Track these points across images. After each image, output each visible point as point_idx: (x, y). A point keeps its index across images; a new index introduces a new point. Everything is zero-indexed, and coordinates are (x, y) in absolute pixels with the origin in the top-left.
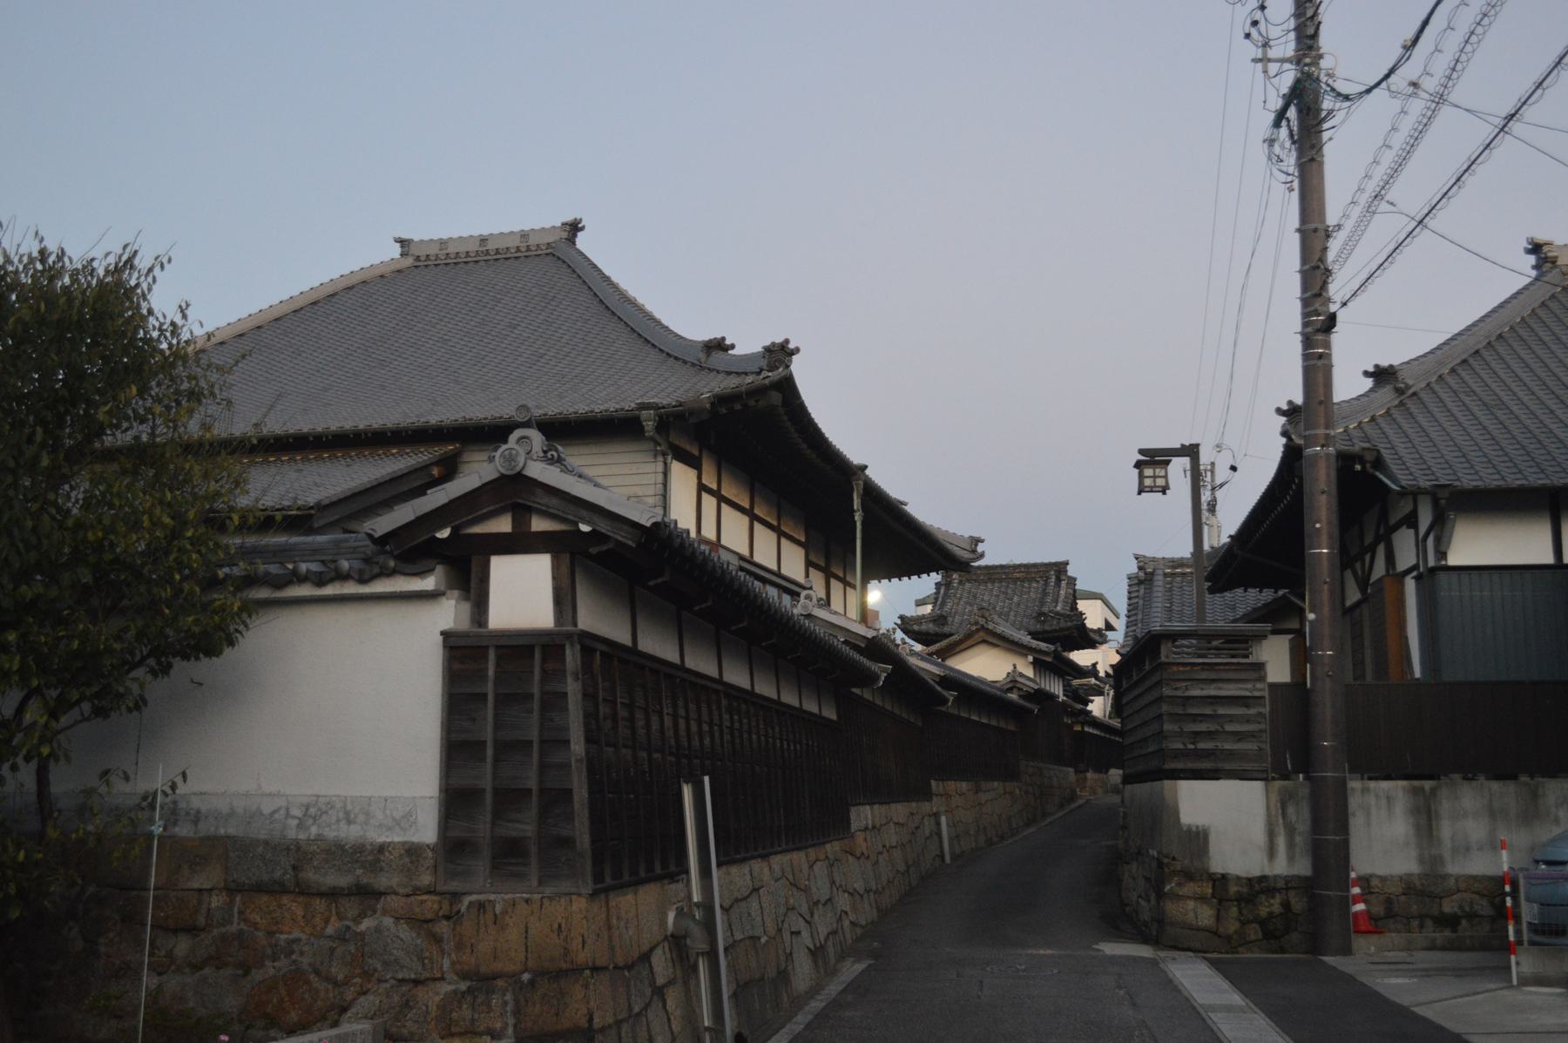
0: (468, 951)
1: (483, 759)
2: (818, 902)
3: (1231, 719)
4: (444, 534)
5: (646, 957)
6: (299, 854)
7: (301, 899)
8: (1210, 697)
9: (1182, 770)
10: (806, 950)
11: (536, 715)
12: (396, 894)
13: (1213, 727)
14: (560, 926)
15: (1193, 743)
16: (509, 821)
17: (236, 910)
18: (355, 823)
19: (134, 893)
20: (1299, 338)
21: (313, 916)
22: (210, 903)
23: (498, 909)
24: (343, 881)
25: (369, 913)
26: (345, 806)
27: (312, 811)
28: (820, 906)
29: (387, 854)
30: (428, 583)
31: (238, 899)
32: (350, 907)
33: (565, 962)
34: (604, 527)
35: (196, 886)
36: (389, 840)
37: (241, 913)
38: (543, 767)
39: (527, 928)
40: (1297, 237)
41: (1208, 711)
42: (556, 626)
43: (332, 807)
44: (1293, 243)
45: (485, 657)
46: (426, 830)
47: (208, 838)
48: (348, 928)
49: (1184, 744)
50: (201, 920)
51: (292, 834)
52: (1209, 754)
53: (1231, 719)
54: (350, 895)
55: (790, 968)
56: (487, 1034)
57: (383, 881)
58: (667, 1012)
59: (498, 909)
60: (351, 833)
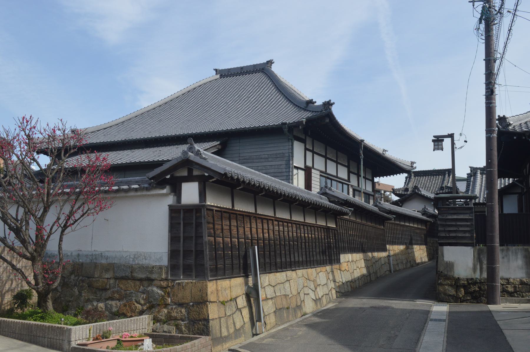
0: (176, 296)
1: (180, 241)
2: (320, 285)
3: (461, 226)
4: (168, 177)
5: (235, 299)
6: (132, 269)
7: (133, 281)
8: (454, 219)
9: (446, 243)
10: (311, 300)
11: (194, 229)
12: (157, 280)
13: (455, 229)
14: (200, 289)
15: (449, 234)
16: (188, 260)
17: (117, 284)
18: (147, 260)
19: (91, 279)
20: (485, 97)
21: (136, 286)
22: (110, 282)
23: (184, 284)
24: (143, 276)
25: (151, 285)
26: (144, 255)
27: (136, 256)
28: (321, 286)
29: (155, 268)
30: (165, 191)
31: (117, 281)
32: (145, 283)
33: (202, 300)
34: (212, 174)
35: (107, 277)
36: (156, 265)
37: (118, 285)
38: (196, 244)
39: (191, 290)
40: (484, 63)
41: (454, 223)
42: (200, 203)
43: (141, 255)
44: (483, 64)
45: (180, 212)
46: (165, 261)
47: (110, 264)
48: (145, 289)
49: (446, 234)
50: (108, 287)
51: (131, 263)
52: (454, 238)
53: (461, 226)
54: (145, 280)
55: (303, 304)
56: (181, 320)
57: (154, 276)
58: (242, 315)
59: (184, 284)
60: (145, 262)
